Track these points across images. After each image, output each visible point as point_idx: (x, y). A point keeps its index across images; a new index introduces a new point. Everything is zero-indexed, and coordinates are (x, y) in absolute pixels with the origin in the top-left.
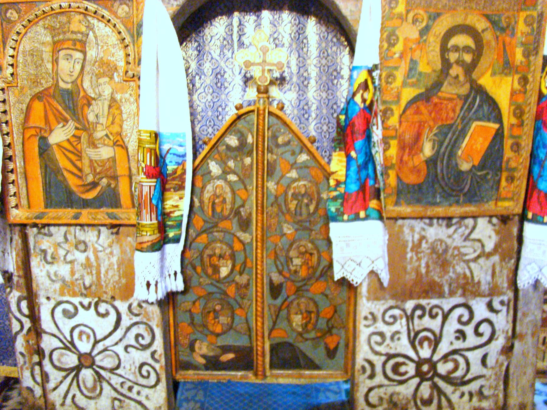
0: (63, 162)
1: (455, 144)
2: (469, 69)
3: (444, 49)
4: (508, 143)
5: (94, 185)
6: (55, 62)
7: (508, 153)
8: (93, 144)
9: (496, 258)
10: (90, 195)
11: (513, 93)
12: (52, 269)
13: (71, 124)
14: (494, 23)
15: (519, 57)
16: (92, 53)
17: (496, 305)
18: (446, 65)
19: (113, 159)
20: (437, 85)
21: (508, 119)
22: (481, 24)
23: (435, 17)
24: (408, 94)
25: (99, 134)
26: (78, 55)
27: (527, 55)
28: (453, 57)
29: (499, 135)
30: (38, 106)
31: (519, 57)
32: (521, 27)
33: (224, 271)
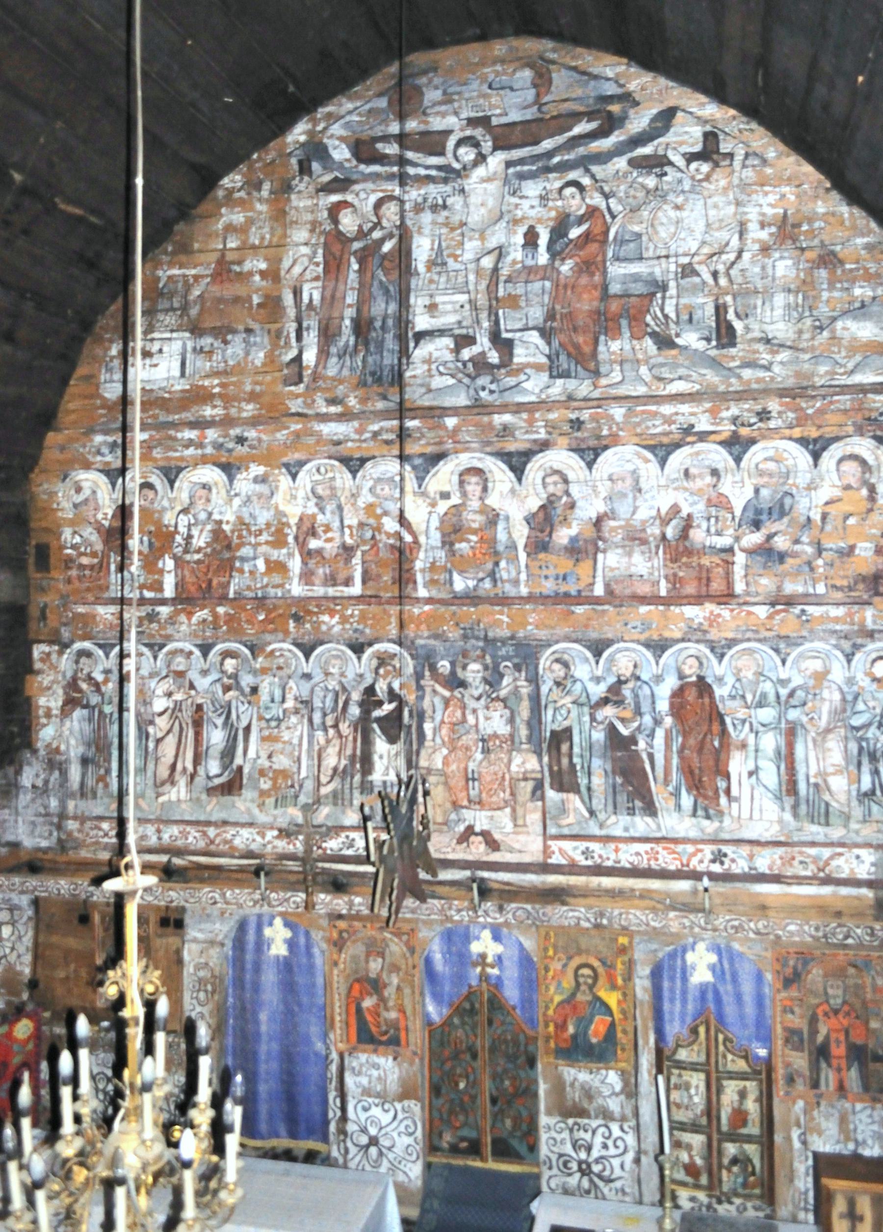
0: (369, 1018)
1: (587, 1028)
2: (591, 987)
3: (576, 976)
4: (619, 1029)
5: (386, 1033)
6: (367, 962)
7: (620, 1035)
8: (387, 1009)
9: (623, 1097)
10: (384, 1038)
11: (619, 1002)
12: (358, 1079)
13: (375, 998)
14: (604, 963)
15: (620, 981)
16: (388, 960)
17: (626, 1128)
18: (578, 984)
19: (398, 1019)
20: (573, 995)
21: (617, 1016)
22: (596, 964)
23: (570, 958)
24: (558, 999)
25: (391, 1004)
26: (380, 960)
27: (624, 980)
28: (581, 980)
29: (612, 1025)
30: (357, 986)
31: (620, 981)
32: (619, 966)
33: (462, 1085)
